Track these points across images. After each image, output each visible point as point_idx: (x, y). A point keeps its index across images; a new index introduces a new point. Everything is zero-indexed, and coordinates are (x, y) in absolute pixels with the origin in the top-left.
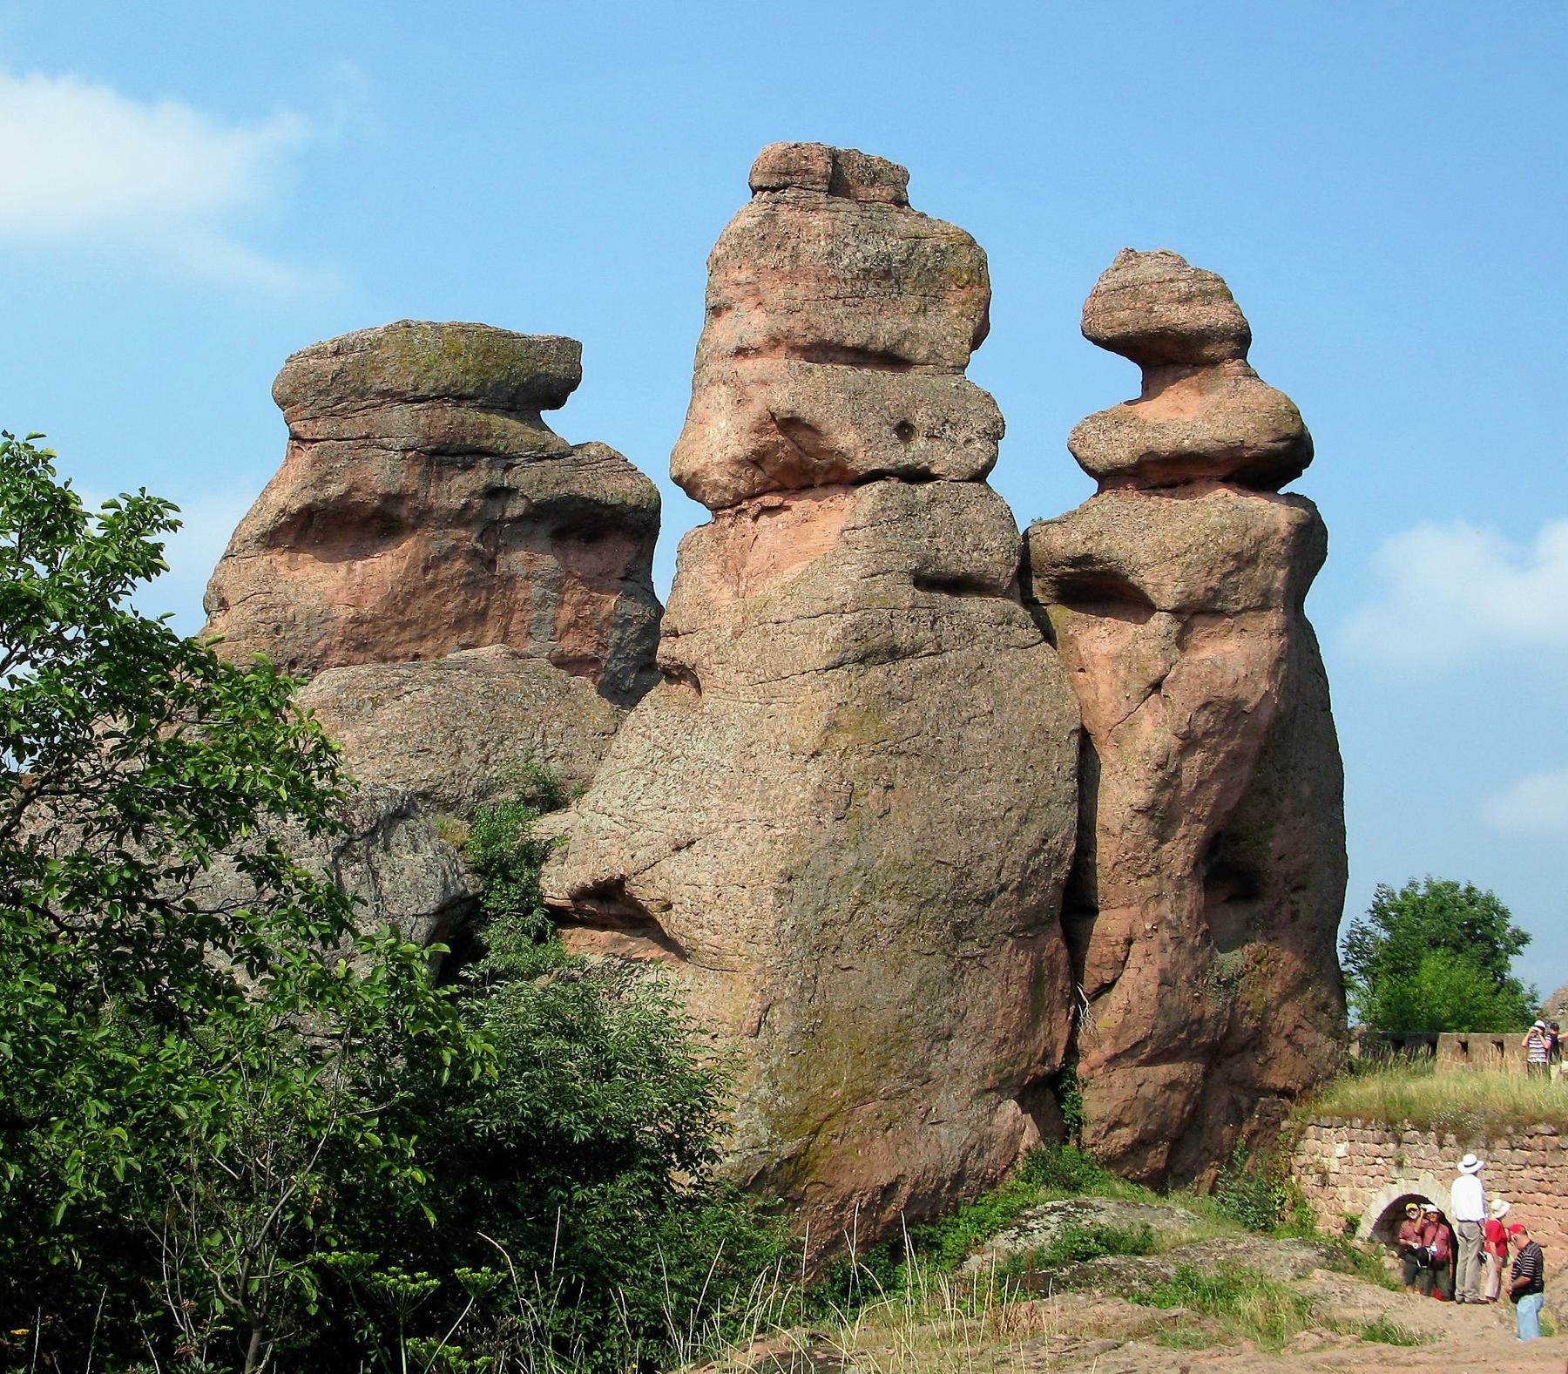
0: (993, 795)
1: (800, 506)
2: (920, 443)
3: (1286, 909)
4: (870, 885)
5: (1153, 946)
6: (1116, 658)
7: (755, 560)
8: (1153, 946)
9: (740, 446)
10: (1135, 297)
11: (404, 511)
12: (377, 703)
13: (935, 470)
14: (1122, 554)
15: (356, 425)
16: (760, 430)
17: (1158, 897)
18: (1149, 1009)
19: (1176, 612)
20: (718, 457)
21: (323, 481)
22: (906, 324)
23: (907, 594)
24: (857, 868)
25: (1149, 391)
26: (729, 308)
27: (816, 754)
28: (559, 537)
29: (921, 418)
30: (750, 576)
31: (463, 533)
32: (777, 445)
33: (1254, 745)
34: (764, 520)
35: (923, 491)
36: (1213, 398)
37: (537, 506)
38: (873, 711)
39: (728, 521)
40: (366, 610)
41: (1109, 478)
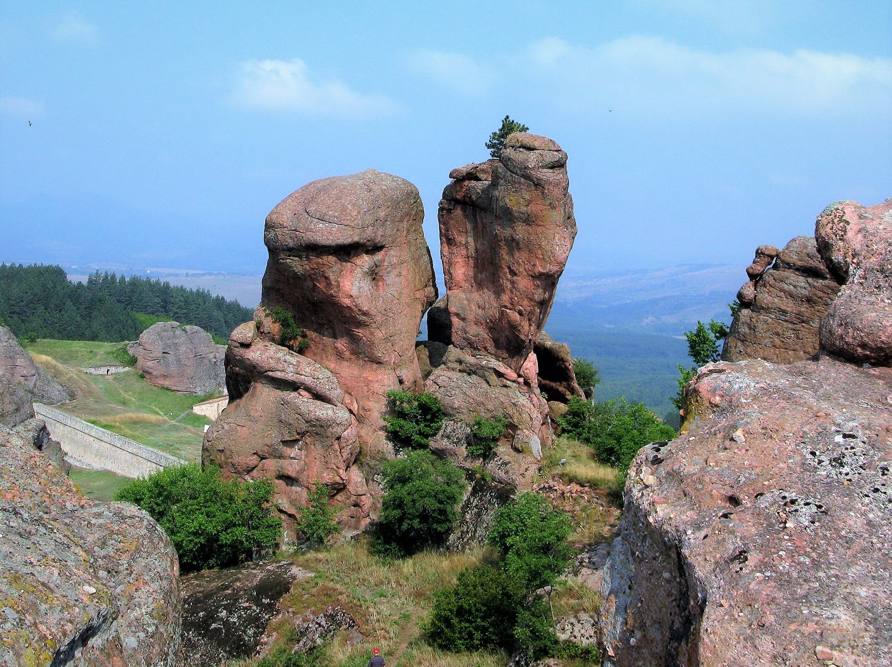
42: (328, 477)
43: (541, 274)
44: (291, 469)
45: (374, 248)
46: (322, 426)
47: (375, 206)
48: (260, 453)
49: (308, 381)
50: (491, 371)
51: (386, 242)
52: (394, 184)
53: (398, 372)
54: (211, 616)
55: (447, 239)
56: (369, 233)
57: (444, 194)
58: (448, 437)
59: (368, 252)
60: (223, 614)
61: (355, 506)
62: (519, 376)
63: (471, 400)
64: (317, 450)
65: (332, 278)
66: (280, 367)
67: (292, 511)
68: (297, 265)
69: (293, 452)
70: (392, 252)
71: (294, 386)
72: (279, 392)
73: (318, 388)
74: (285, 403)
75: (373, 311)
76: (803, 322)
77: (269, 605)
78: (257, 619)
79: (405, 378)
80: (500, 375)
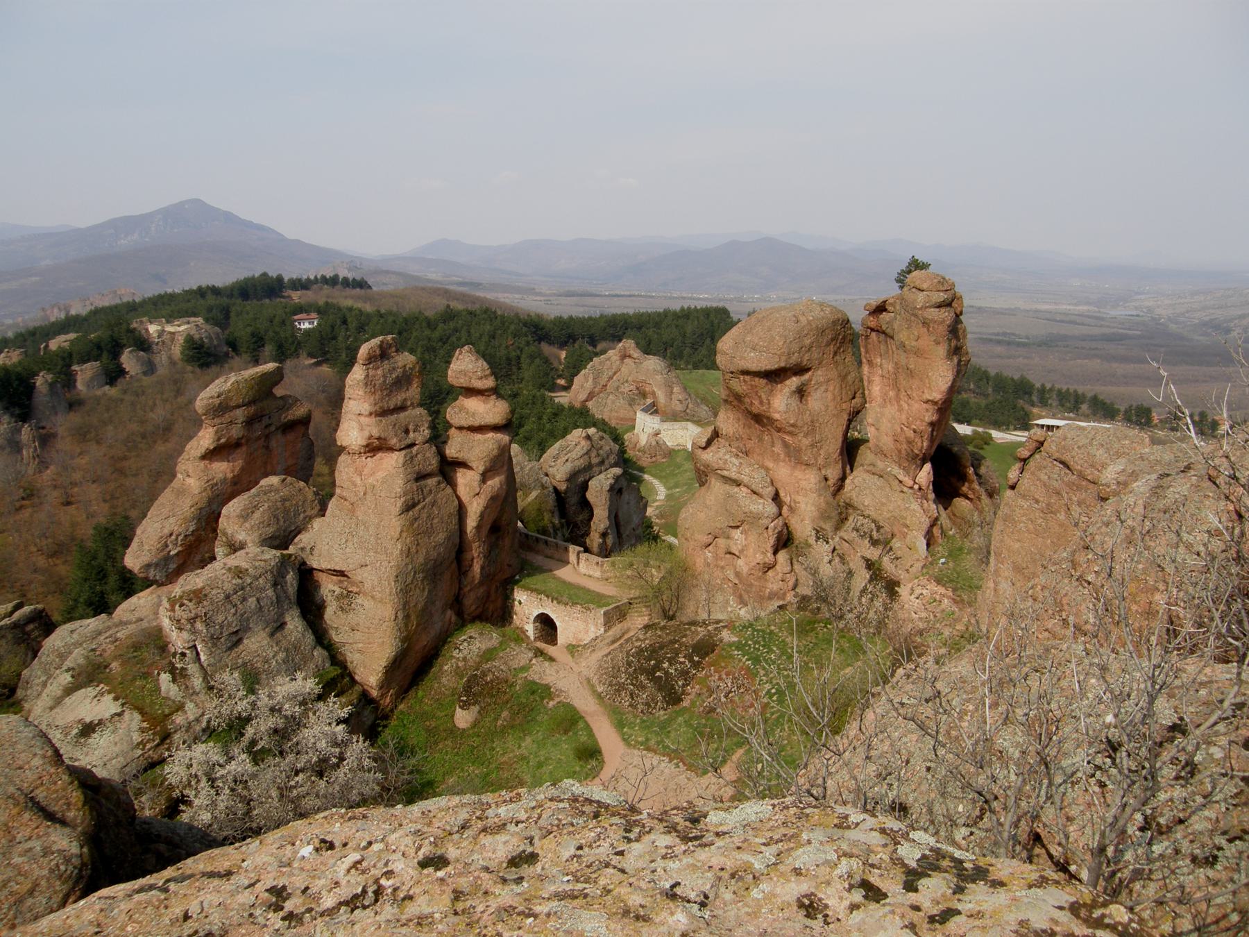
0: (441, 537)
1: (379, 455)
2: (411, 435)
4: (415, 572)
6: (466, 485)
7: (366, 471)
10: (465, 375)
11: (243, 441)
12: (253, 512)
16: (369, 439)
21: (219, 439)
29: (411, 427)
36: (489, 406)
38: (412, 524)
42: (759, 558)
45: (800, 370)
47: (800, 337)
49: (746, 479)
52: (822, 313)
53: (823, 472)
54: (657, 667)
56: (794, 359)
58: (857, 531)
60: (666, 665)
65: (764, 396)
69: (737, 534)
70: (819, 372)
71: (738, 484)
74: (730, 496)
75: (800, 423)
76: (1052, 512)
77: (698, 662)
78: (687, 673)
79: (830, 476)
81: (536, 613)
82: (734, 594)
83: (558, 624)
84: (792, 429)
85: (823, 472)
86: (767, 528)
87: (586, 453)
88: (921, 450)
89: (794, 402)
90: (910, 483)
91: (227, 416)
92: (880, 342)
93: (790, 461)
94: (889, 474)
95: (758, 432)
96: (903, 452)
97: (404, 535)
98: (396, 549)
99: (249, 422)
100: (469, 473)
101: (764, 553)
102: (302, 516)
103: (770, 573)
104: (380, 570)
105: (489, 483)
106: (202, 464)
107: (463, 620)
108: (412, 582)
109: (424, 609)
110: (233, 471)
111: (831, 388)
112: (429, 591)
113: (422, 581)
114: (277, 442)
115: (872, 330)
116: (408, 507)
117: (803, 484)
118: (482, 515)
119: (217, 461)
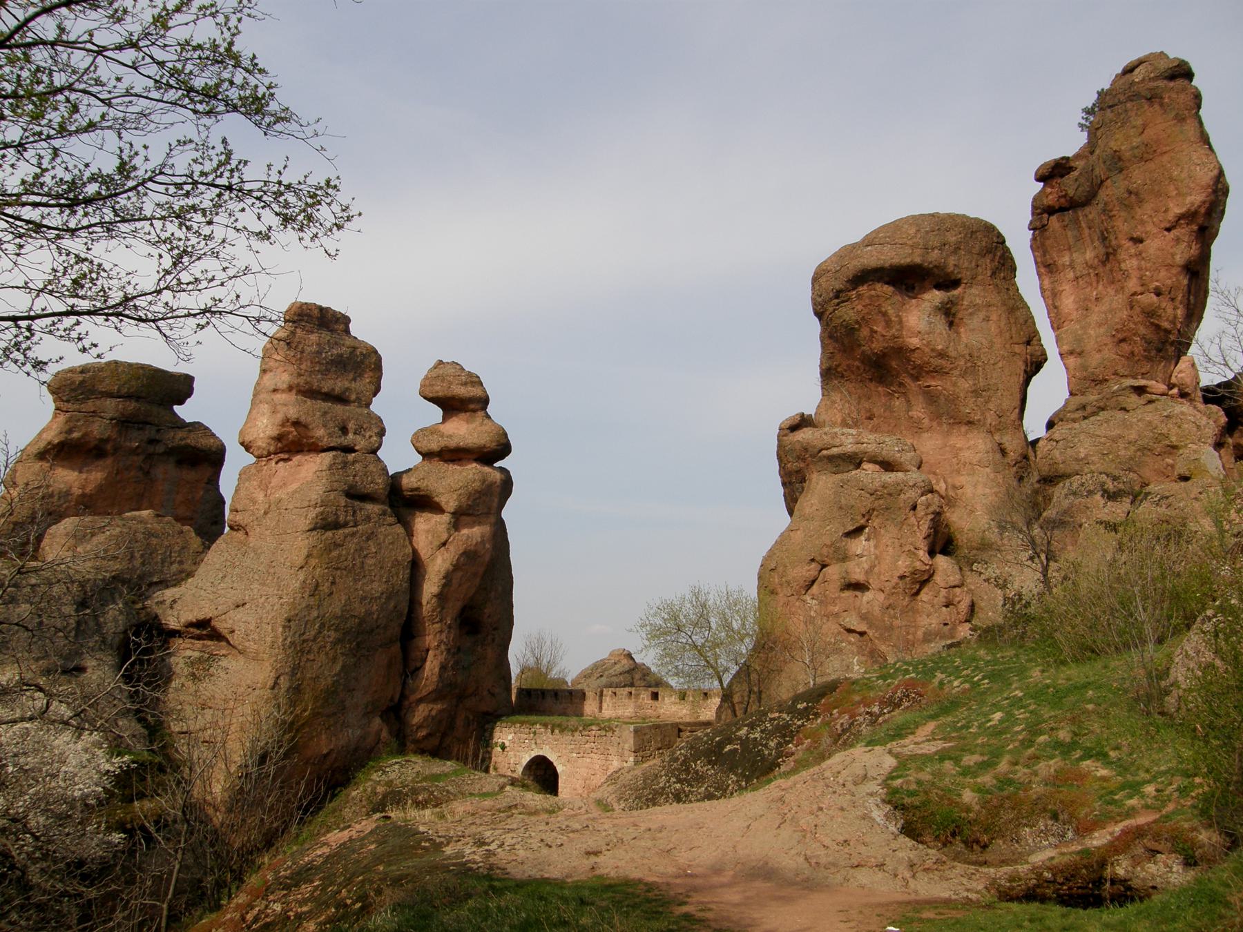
0: (377, 588)
1: (297, 459)
2: (351, 436)
3: (490, 637)
4: (322, 625)
5: (438, 652)
6: (428, 531)
7: (275, 481)
8: (438, 652)
9: (272, 431)
10: (443, 381)
11: (109, 447)
12: (93, 535)
13: (357, 448)
14: (432, 489)
15: (90, 405)
16: (283, 425)
17: (441, 632)
18: (435, 679)
19: (453, 513)
20: (262, 435)
21: (70, 431)
22: (347, 384)
23: (343, 501)
24: (318, 617)
25: (445, 419)
26: (271, 371)
27: (302, 568)
28: (179, 463)
29: (351, 426)
30: (272, 488)
31: (136, 458)
32: (289, 433)
33: (481, 570)
34: (281, 464)
35: (351, 457)
36: (474, 425)
37: (171, 448)
38: (328, 550)
39: (264, 463)
40: (88, 491)
41: (427, 455)
42: (903, 565)
43: (1181, 217)
44: (858, 570)
45: (948, 283)
46: (890, 495)
48: (818, 558)
49: (871, 448)
50: (1127, 392)
51: (965, 275)
55: (1047, 267)
57: (1034, 207)
59: (938, 287)
61: (947, 606)
62: (1171, 386)
63: (1103, 440)
64: (889, 535)
65: (891, 311)
66: (837, 442)
67: (862, 627)
68: (848, 313)
69: (859, 545)
70: (974, 291)
71: (855, 461)
72: (839, 476)
73: (884, 453)
75: (953, 354)
79: (1008, 446)
80: (1140, 390)
81: (526, 759)
82: (860, 652)
83: (559, 769)
84: (939, 362)
85: (997, 437)
86: (914, 508)
87: (628, 672)
88: (1173, 322)
89: (940, 324)
90: (1162, 387)
91: (90, 402)
92: (1065, 227)
93: (940, 424)
94: (1116, 394)
95: (883, 400)
96: (1139, 349)
97: (313, 562)
98: (295, 582)
99: (125, 423)
100: (437, 518)
101: (912, 554)
102: (175, 567)
103: (925, 595)
104: (263, 607)
105: (465, 531)
106: (37, 466)
107: (402, 743)
108: (315, 639)
109: (331, 693)
110: (83, 487)
111: (994, 317)
112: (343, 667)
113: (334, 644)
114: (165, 472)
115: (1051, 211)
116: (326, 524)
117: (966, 455)
118: (448, 578)
119: (63, 466)
